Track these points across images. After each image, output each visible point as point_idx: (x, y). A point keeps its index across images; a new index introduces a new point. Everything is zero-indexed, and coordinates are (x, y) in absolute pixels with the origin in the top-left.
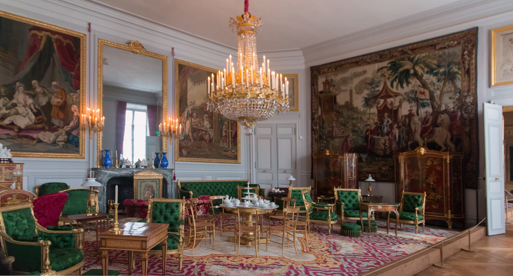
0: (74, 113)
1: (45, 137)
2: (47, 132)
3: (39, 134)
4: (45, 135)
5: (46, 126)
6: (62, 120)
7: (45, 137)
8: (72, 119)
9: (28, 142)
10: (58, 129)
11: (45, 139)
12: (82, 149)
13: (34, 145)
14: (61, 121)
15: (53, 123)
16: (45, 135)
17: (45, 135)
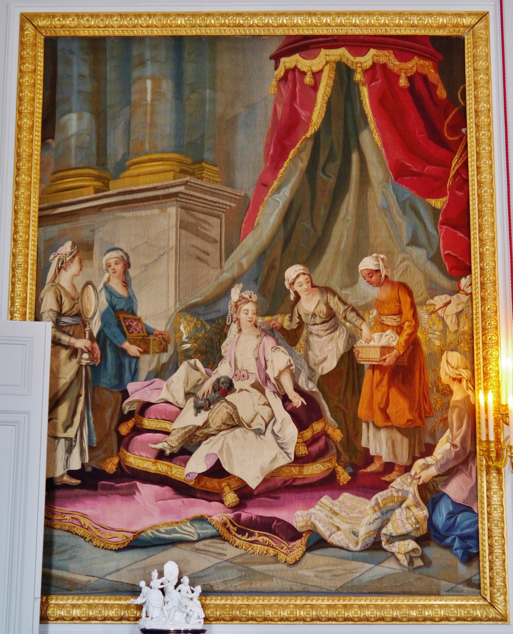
0: (451, 392)
1: (336, 521)
2: (346, 496)
3: (312, 510)
4: (336, 509)
5: (340, 469)
6: (403, 431)
7: (336, 521)
8: (445, 423)
9: (271, 551)
10: (386, 478)
11: (338, 529)
12: (491, 553)
13: (297, 562)
14: (398, 436)
15: (367, 450)
16: (336, 514)
17: (336, 514)
